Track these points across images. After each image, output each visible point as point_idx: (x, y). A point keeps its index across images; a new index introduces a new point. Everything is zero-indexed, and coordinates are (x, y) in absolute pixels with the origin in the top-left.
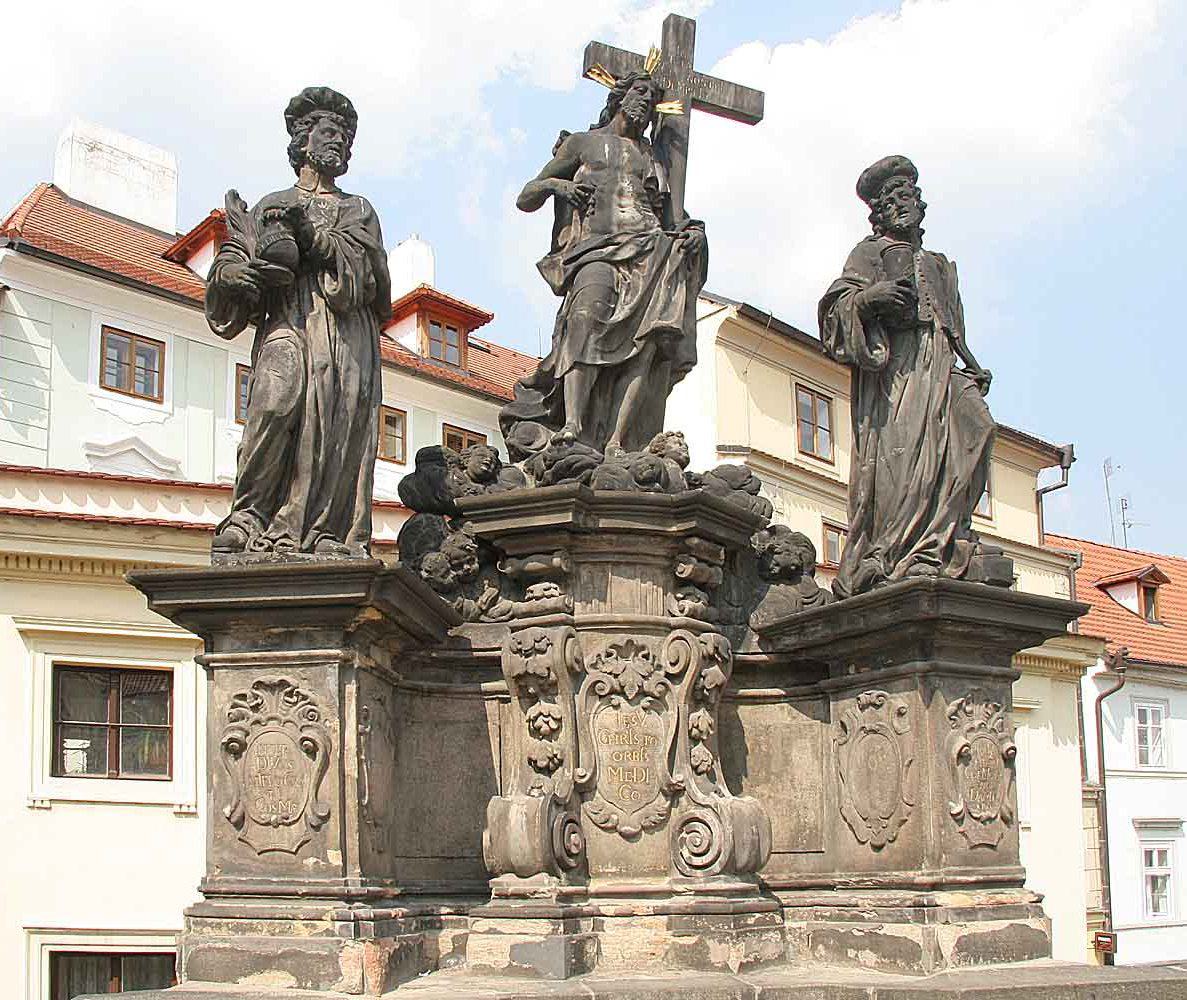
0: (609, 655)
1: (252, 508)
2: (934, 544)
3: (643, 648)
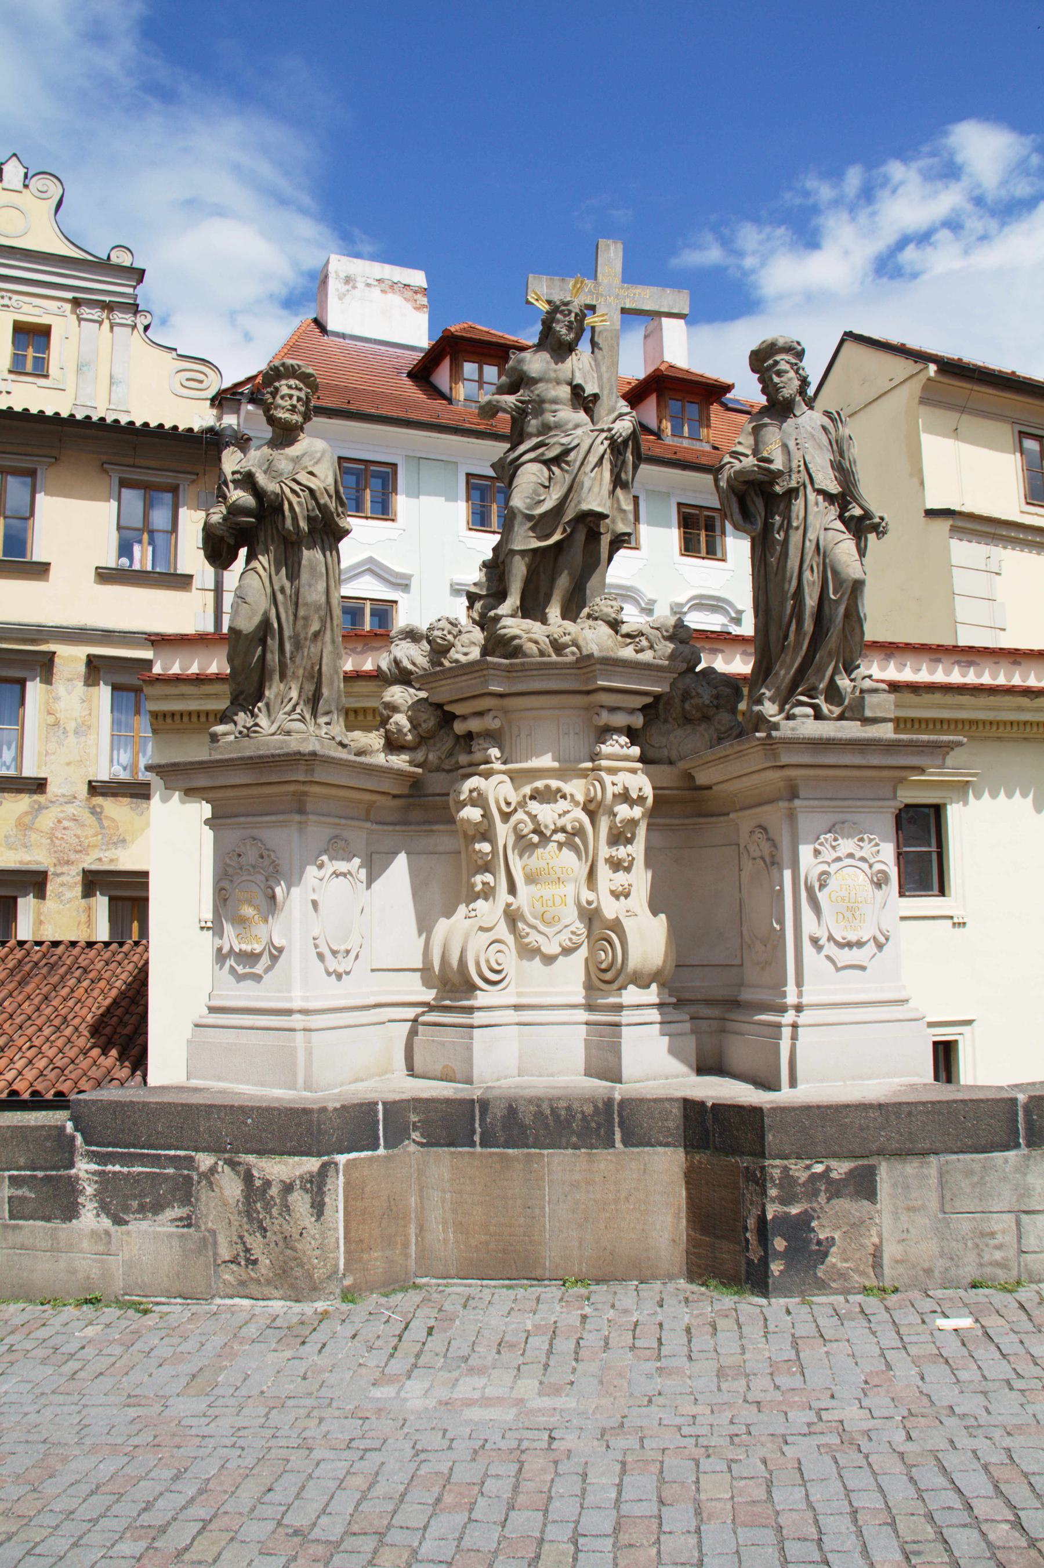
0: (532, 797)
3: (559, 790)
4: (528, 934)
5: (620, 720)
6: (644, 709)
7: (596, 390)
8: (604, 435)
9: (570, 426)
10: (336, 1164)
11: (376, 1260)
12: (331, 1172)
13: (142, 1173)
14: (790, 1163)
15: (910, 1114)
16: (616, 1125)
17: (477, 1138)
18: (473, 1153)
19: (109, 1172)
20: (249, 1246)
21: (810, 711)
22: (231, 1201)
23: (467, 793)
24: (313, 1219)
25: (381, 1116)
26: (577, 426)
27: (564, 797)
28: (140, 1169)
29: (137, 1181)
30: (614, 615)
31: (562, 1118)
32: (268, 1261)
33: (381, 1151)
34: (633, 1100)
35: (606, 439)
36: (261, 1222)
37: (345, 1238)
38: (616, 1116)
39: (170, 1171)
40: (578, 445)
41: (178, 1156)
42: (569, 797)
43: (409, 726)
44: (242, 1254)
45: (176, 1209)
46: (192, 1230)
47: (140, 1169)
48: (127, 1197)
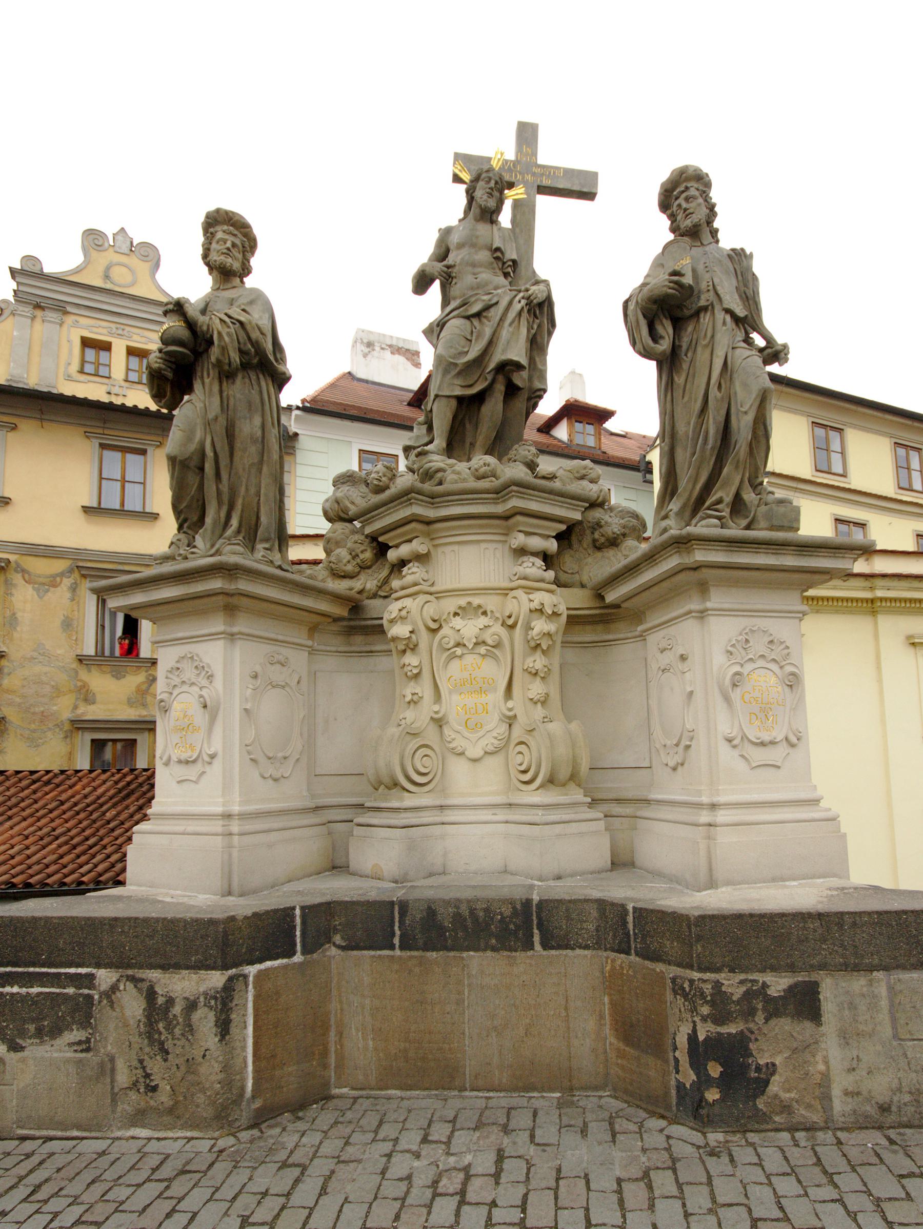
0: (456, 614)
1: (185, 530)
2: (720, 501)
3: (479, 606)
4: (454, 739)
5: (536, 543)
6: (559, 537)
7: (514, 257)
8: (521, 295)
9: (491, 287)
10: (245, 977)
11: (290, 1077)
12: (239, 985)
13: (41, 993)
14: (721, 977)
15: (854, 924)
16: (535, 927)
17: (396, 941)
18: (393, 957)
19: (7, 994)
20: (149, 1072)
21: (716, 521)
22: (132, 1022)
23: (397, 611)
24: (217, 1039)
26: (496, 288)
27: (485, 613)
28: (40, 990)
29: (35, 1003)
30: (530, 457)
31: (481, 920)
32: (168, 1087)
33: (298, 958)
34: (551, 901)
35: (523, 298)
36: (162, 1043)
37: (255, 1055)
38: (534, 918)
39: (71, 991)
40: (497, 303)
41: (80, 974)
42: (489, 613)
43: (349, 557)
44: (142, 1080)
45: (75, 1032)
46: (89, 1055)
47: (40, 990)
48: (25, 1022)
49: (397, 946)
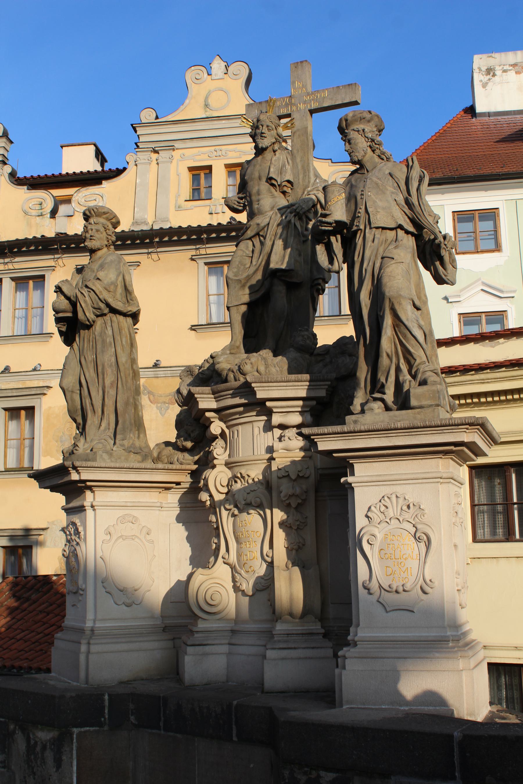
17: (162, 724)
24: (55, 770)
25: (107, 703)
49: (162, 728)
